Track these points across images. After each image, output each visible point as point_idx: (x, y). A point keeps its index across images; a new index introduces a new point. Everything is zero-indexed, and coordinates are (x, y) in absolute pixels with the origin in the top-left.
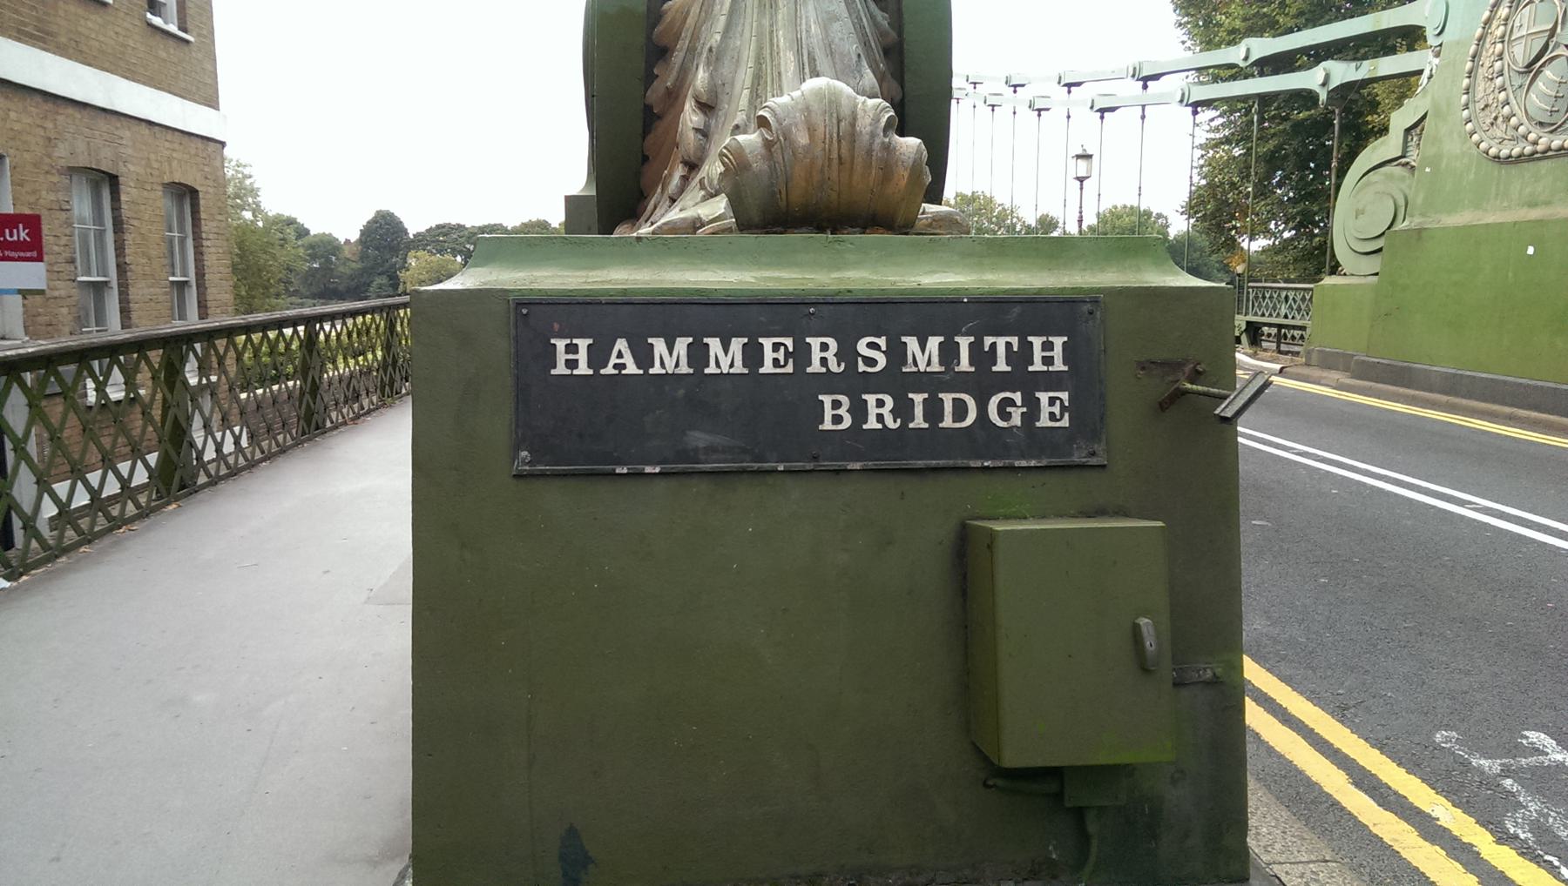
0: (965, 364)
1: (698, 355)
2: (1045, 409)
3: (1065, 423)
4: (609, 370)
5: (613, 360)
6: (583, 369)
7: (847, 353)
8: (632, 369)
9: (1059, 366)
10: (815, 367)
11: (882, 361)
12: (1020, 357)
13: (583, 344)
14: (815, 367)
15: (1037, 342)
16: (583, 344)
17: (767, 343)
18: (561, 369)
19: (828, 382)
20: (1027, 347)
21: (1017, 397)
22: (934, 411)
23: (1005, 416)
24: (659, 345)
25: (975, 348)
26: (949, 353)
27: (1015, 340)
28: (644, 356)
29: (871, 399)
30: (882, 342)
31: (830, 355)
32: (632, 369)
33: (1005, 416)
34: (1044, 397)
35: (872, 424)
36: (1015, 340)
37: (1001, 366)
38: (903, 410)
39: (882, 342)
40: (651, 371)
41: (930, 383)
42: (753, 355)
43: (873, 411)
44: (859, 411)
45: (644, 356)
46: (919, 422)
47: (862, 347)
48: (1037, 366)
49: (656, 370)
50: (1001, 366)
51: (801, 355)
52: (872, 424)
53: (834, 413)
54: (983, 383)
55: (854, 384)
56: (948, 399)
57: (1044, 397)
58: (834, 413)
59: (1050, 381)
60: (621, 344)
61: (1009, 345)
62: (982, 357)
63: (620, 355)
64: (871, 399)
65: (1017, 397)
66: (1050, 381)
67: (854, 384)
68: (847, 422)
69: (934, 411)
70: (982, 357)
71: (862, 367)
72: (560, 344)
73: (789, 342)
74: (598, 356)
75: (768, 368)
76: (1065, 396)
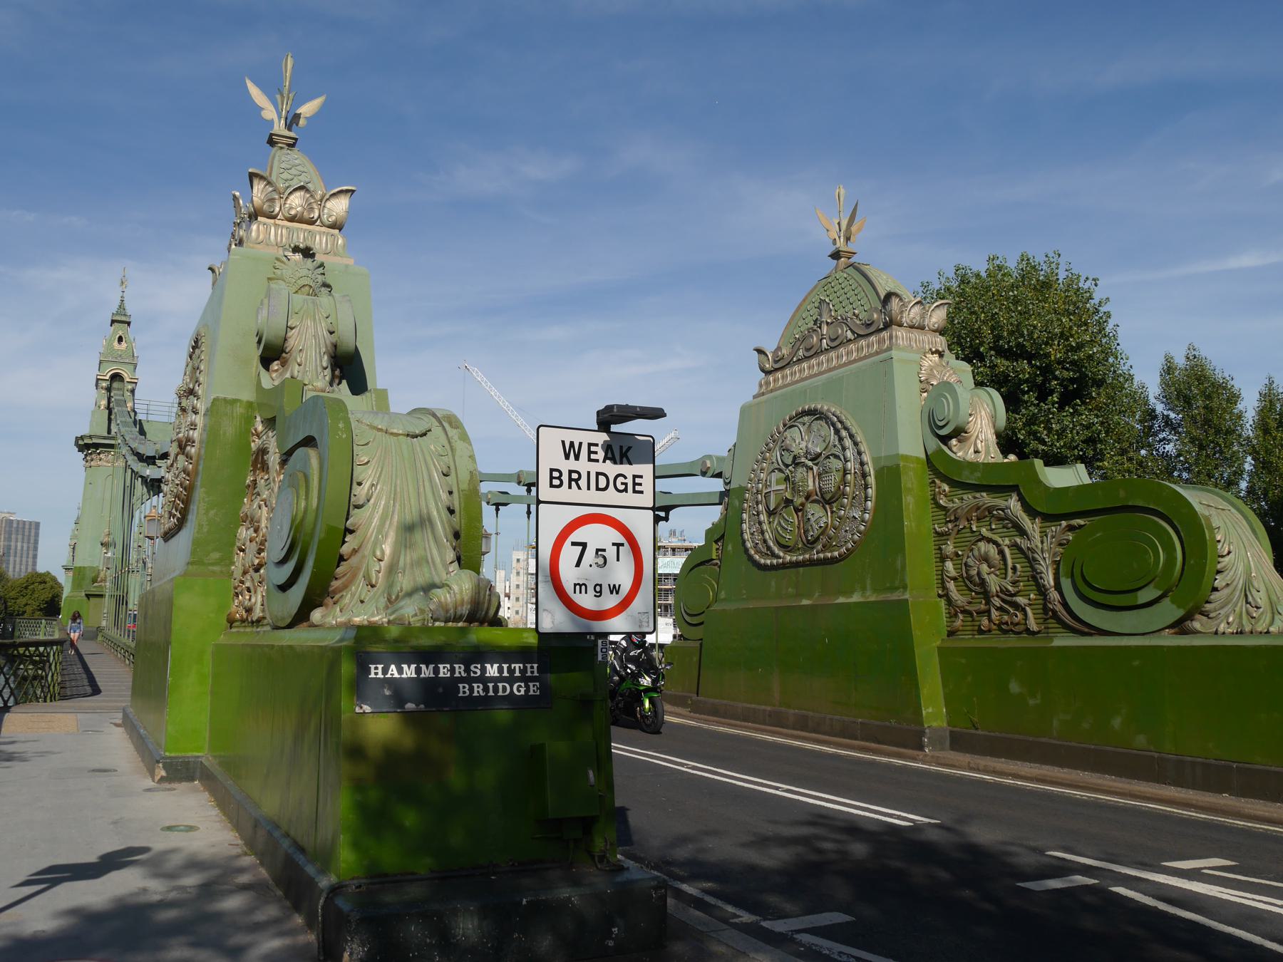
0: (506, 674)
2: (532, 688)
3: (538, 693)
4: (388, 676)
5: (390, 672)
6: (380, 676)
7: (467, 670)
8: (396, 675)
9: (536, 674)
10: (457, 675)
11: (479, 673)
12: (523, 671)
13: (380, 667)
14: (457, 675)
15: (529, 666)
16: (380, 667)
17: (441, 666)
18: (372, 676)
19: (462, 680)
20: (525, 668)
21: (523, 684)
23: (519, 691)
24: (405, 667)
25: (509, 668)
26: (500, 670)
27: (521, 665)
28: (400, 671)
29: (475, 685)
30: (479, 666)
31: (462, 670)
32: (396, 675)
33: (519, 691)
34: (531, 684)
35: (476, 694)
36: (521, 665)
37: (517, 674)
38: (486, 689)
39: (479, 666)
40: (403, 676)
41: (495, 680)
42: (436, 671)
43: (476, 689)
44: (471, 689)
45: (400, 671)
46: (491, 693)
47: (472, 667)
48: (529, 674)
49: (404, 676)
50: (517, 674)
51: (452, 670)
52: (476, 694)
53: (463, 689)
54: (511, 680)
55: (469, 680)
56: (500, 685)
57: (531, 684)
58: (463, 689)
59: (533, 679)
60: (393, 667)
61: (520, 667)
62: (511, 671)
63: (392, 671)
64: (475, 685)
65: (523, 684)
66: (533, 679)
67: (469, 680)
68: (468, 693)
70: (511, 671)
71: (472, 675)
72: (372, 667)
73: (448, 666)
74: (385, 671)
75: (441, 675)
76: (538, 684)
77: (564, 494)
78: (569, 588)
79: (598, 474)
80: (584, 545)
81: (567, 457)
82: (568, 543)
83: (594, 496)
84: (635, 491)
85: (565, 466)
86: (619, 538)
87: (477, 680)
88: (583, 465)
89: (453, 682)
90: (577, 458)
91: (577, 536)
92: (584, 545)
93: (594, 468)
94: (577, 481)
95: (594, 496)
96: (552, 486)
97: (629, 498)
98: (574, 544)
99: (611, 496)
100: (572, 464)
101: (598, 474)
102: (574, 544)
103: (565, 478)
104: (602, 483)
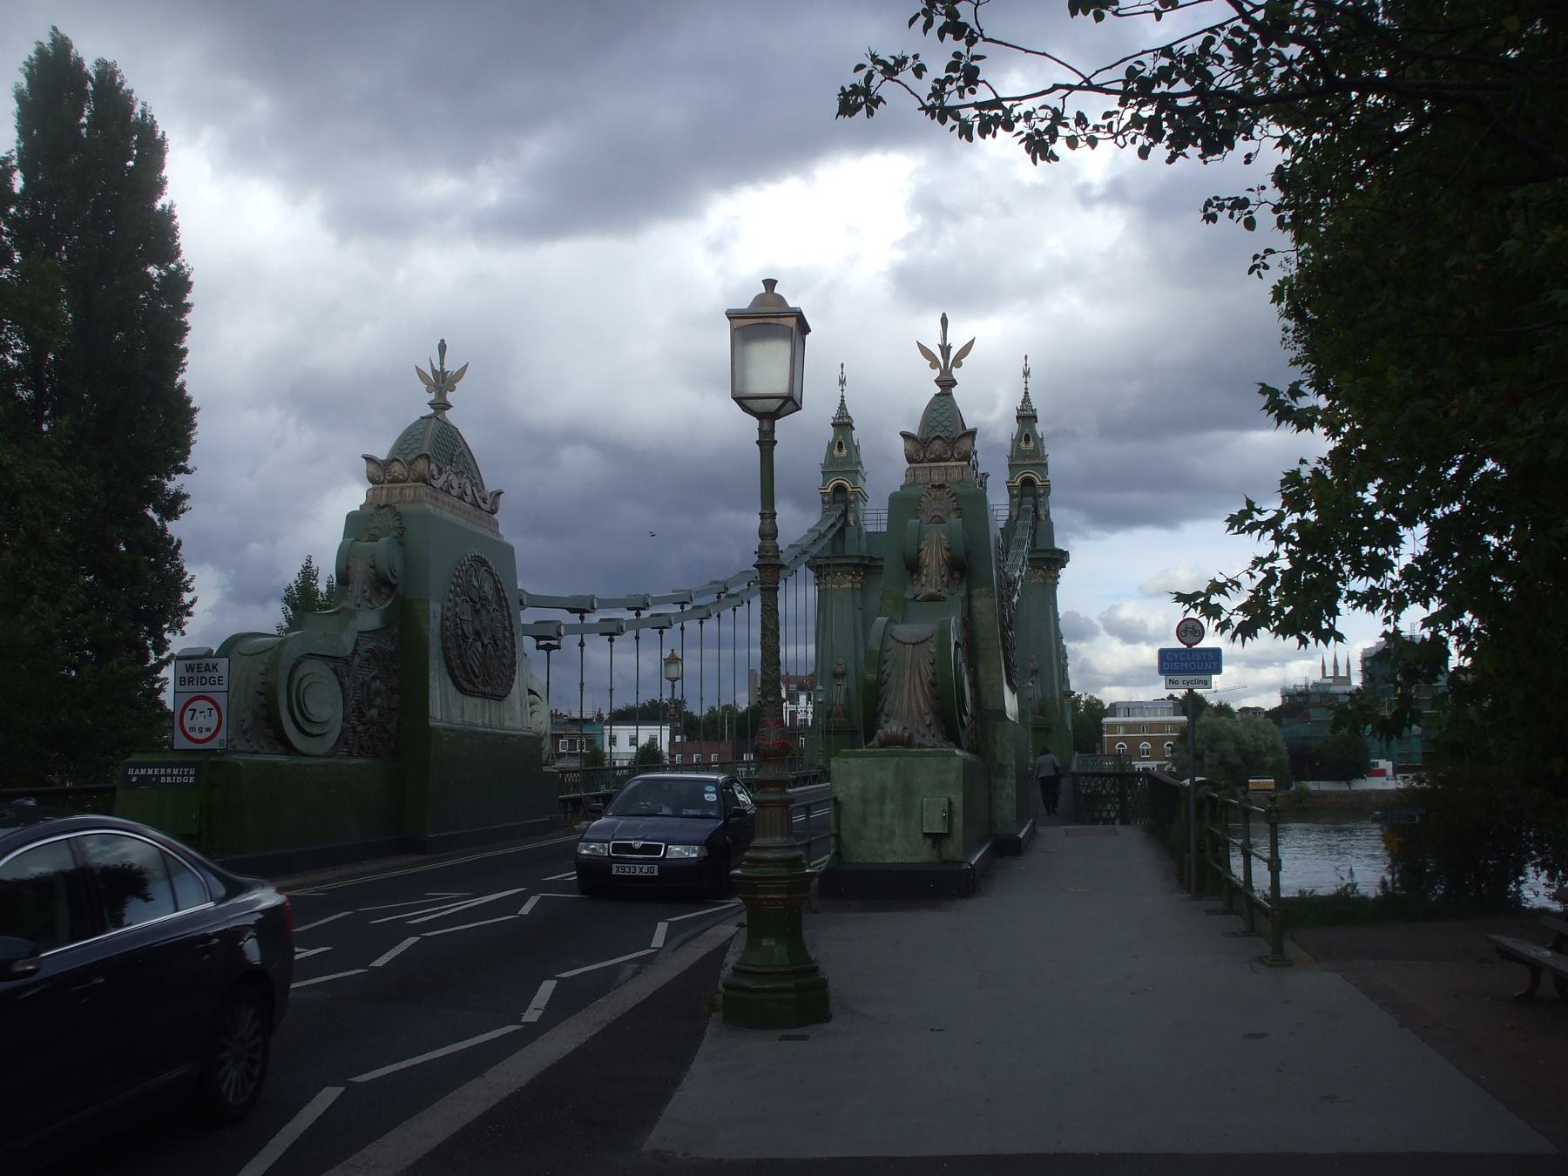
1: (147, 771)
19: (163, 775)
22: (176, 780)
26: (179, 771)
28: (140, 772)
38: (172, 780)
45: (140, 772)
51: (160, 771)
54: (183, 776)
55: (166, 776)
59: (191, 775)
62: (183, 772)
66: (191, 775)
69: (176, 780)
70: (183, 772)
77: (187, 688)
78: (187, 730)
79: (202, 678)
80: (194, 710)
81: (188, 671)
82: (187, 711)
83: (199, 688)
84: (219, 684)
85: (187, 675)
86: (211, 706)
87: (168, 776)
88: (195, 674)
89: (159, 777)
90: (192, 671)
91: (192, 706)
92: (194, 710)
93: (200, 675)
94: (192, 681)
95: (199, 688)
96: (181, 685)
97: (217, 687)
98: (190, 710)
99: (208, 687)
100: (190, 674)
101: (202, 678)
102: (190, 710)
103: (187, 681)
104: (204, 682)
